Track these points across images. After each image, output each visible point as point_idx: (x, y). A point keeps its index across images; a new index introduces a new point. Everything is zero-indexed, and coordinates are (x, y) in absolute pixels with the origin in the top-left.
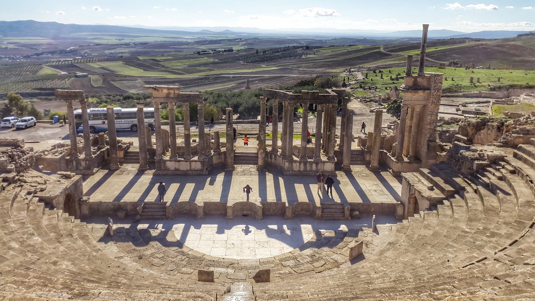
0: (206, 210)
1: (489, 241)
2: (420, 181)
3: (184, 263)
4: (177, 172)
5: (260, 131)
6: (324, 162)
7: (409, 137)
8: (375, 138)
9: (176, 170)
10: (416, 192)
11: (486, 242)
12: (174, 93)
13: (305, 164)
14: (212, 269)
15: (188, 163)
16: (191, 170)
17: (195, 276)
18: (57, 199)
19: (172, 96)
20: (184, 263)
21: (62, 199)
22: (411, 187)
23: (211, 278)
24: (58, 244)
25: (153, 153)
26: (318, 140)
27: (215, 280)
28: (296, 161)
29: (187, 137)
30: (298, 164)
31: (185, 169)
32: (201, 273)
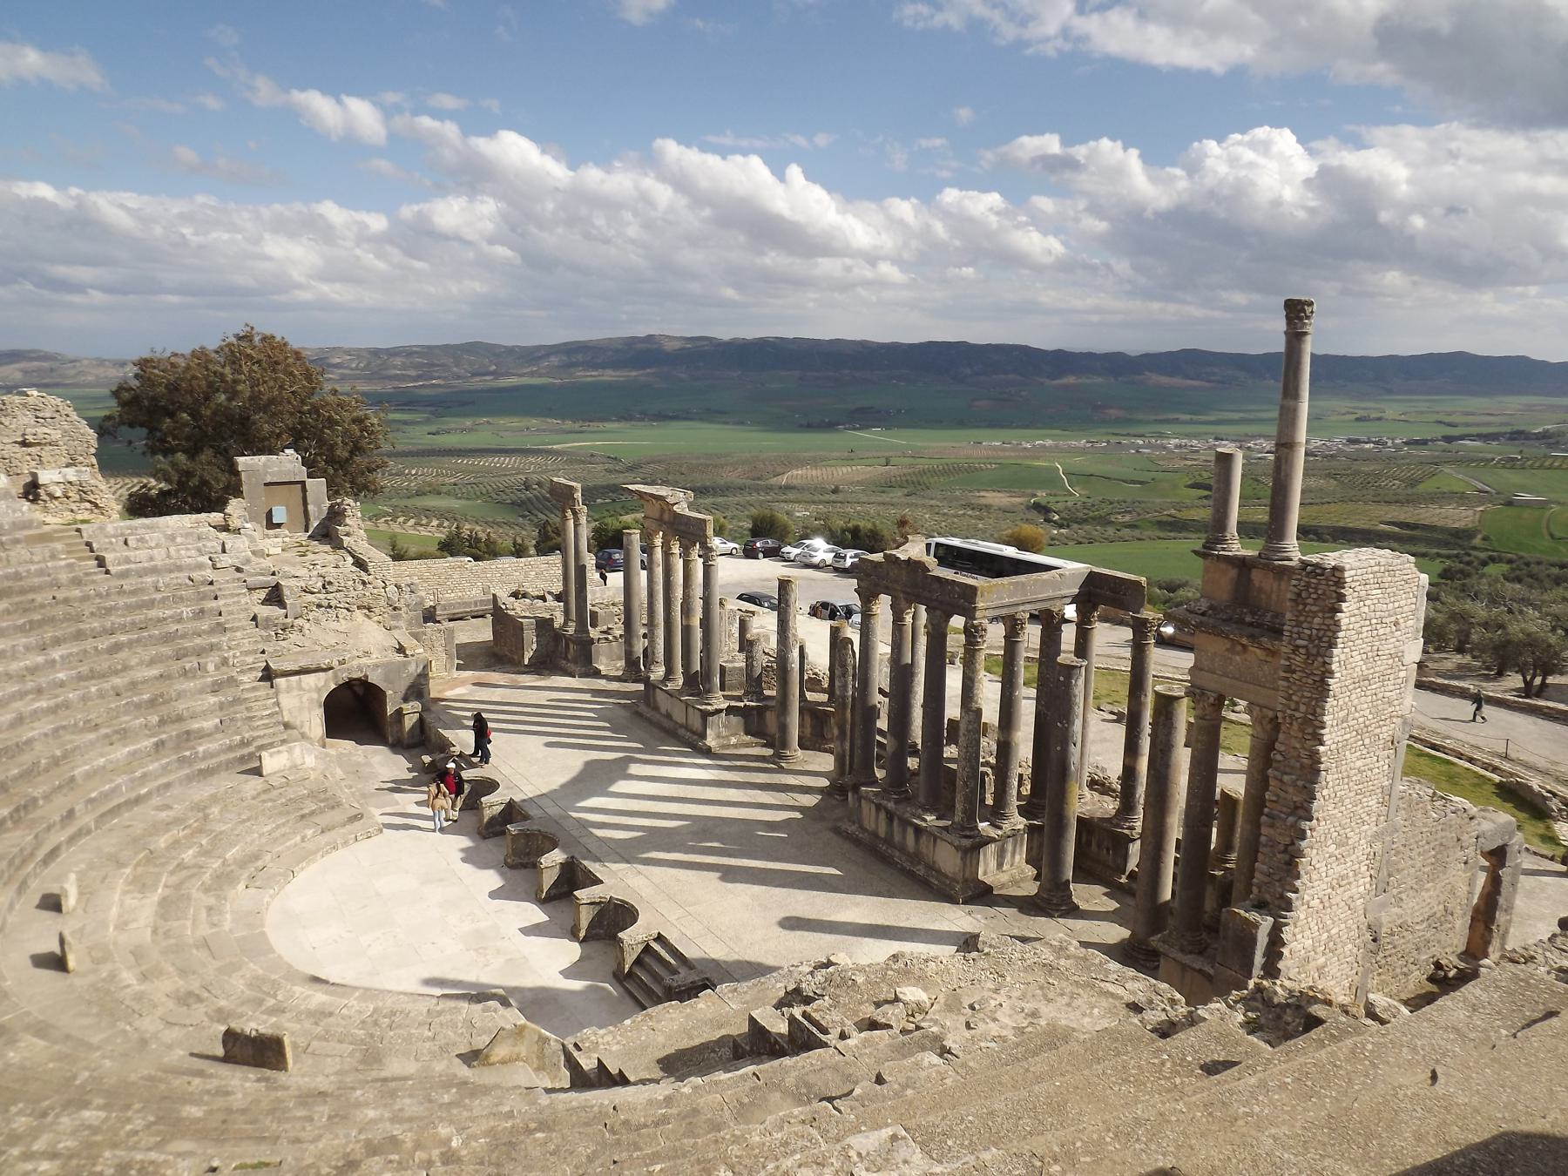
13: (890, 816)
16: (687, 727)
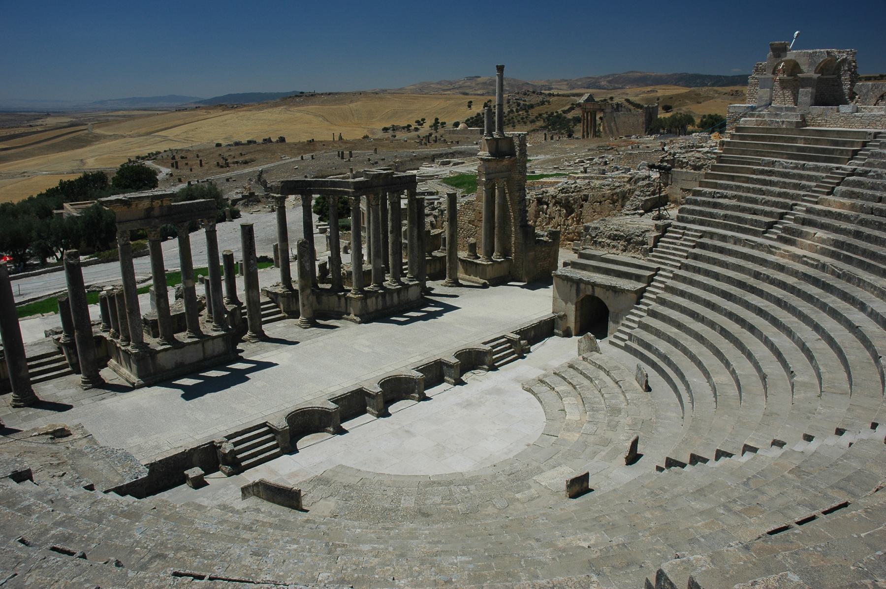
12: (161, 206)
15: (200, 345)
19: (156, 212)
22: (582, 286)
30: (374, 299)
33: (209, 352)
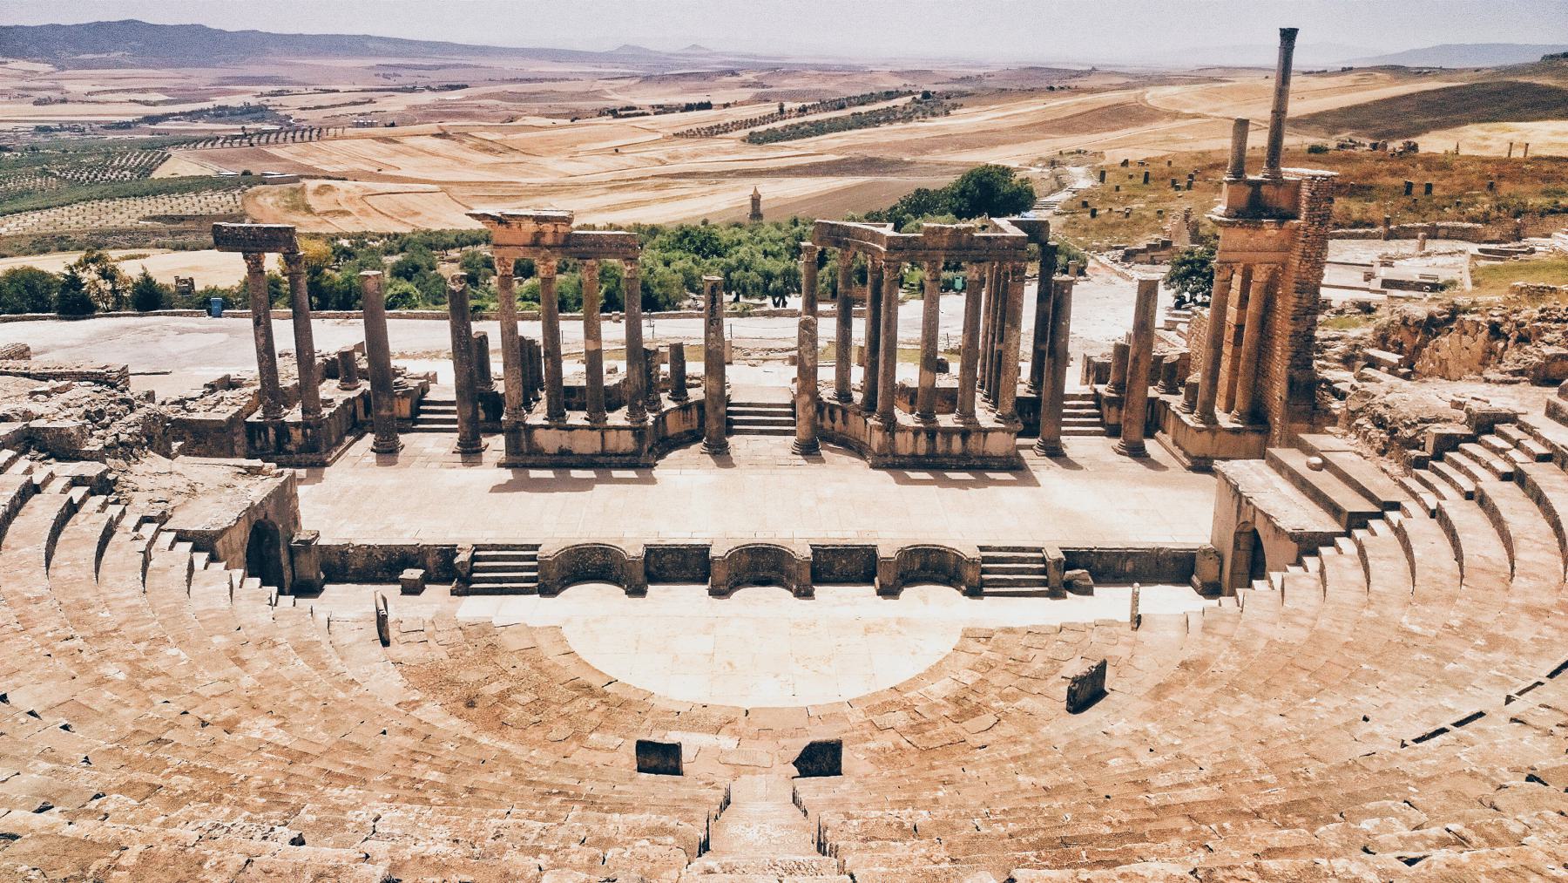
0: (652, 569)
1: (1484, 662)
2: (1269, 484)
3: (594, 718)
4: (566, 460)
5: (801, 343)
6: (986, 431)
7: (1236, 357)
8: (1136, 360)
9: (563, 452)
10: (1258, 515)
11: (1473, 664)
12: (555, 232)
14: (671, 738)
15: (597, 434)
17: (627, 756)
18: (226, 538)
19: (548, 240)
20: (594, 718)
21: (240, 537)
23: (672, 763)
24: (236, 669)
25: (495, 404)
26: (968, 368)
27: (685, 767)
28: (904, 429)
29: (593, 361)
30: (910, 435)
31: (588, 451)
32: (644, 748)
33: (610, 445)
